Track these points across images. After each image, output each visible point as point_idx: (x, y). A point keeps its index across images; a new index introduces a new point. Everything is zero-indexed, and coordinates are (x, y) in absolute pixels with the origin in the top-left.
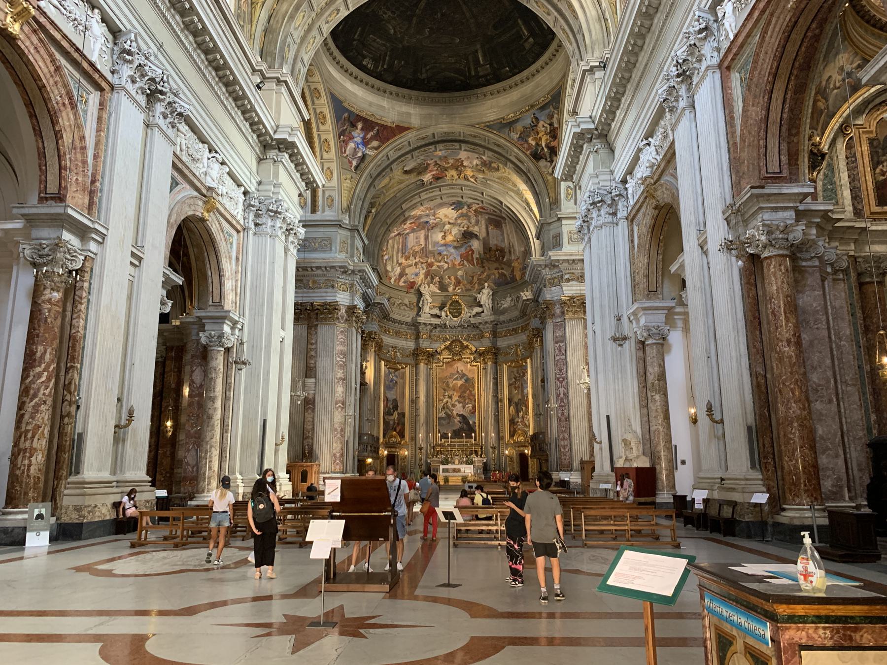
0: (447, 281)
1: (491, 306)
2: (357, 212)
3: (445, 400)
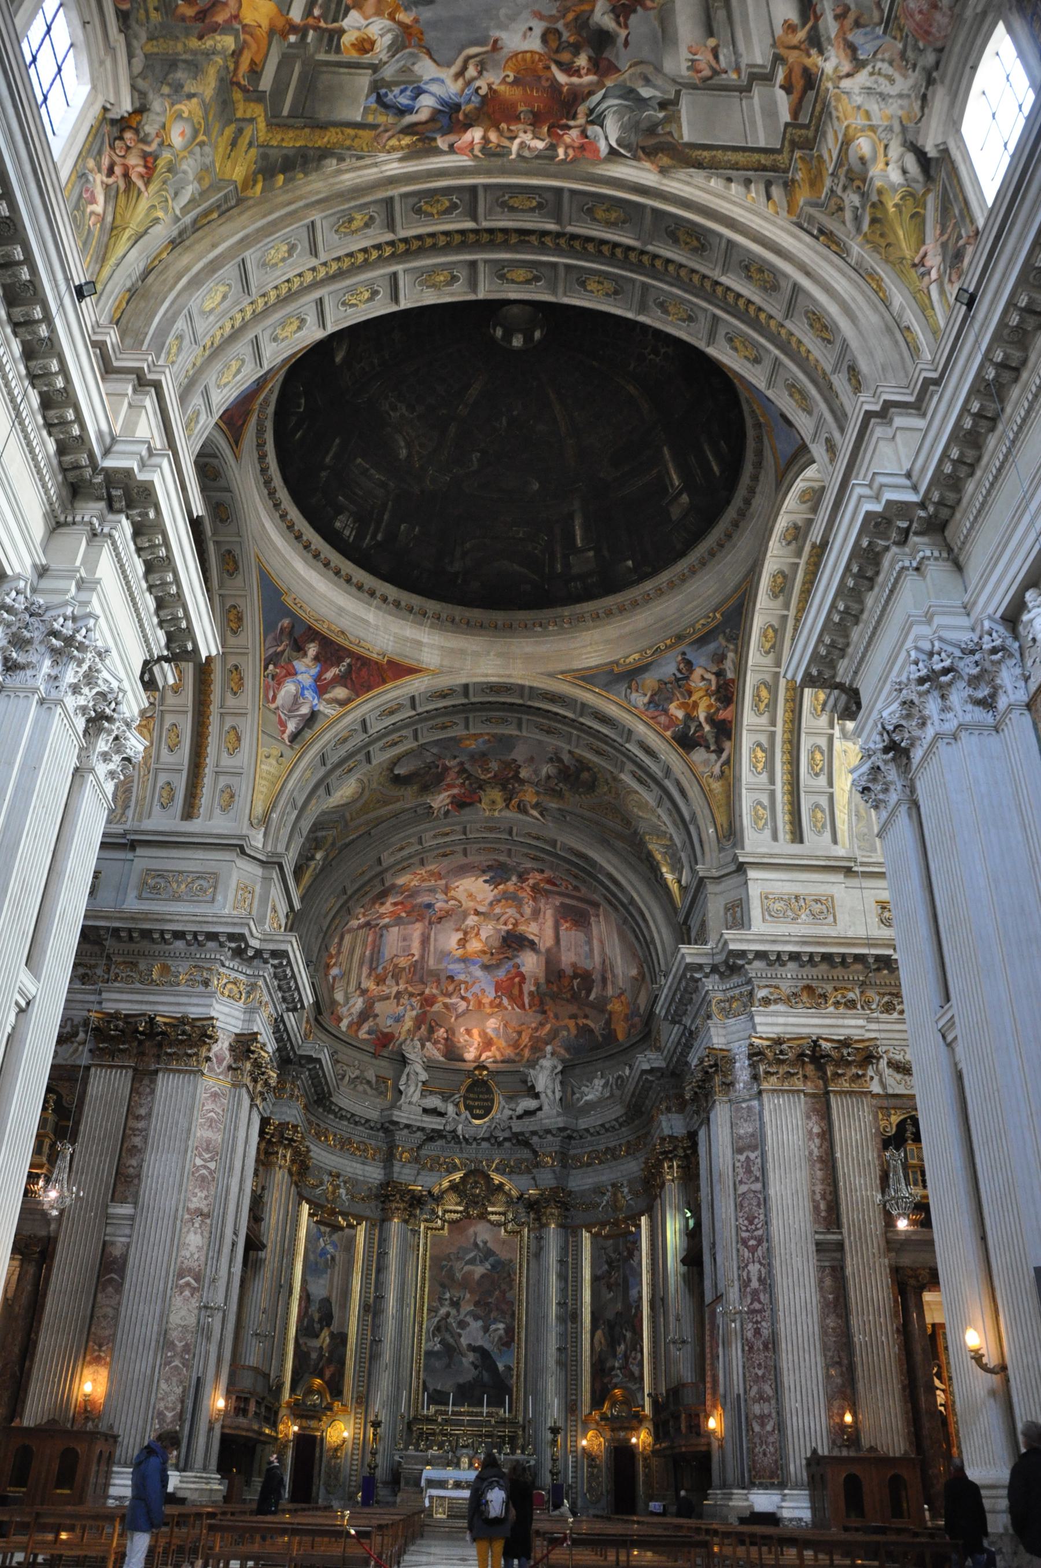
0: (462, 1038)
1: (558, 1095)
2: (285, 832)
3: (443, 1311)
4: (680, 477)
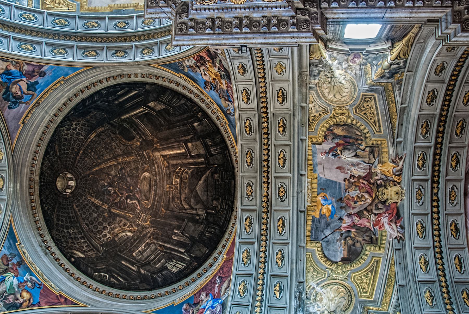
4: (139, 109)
